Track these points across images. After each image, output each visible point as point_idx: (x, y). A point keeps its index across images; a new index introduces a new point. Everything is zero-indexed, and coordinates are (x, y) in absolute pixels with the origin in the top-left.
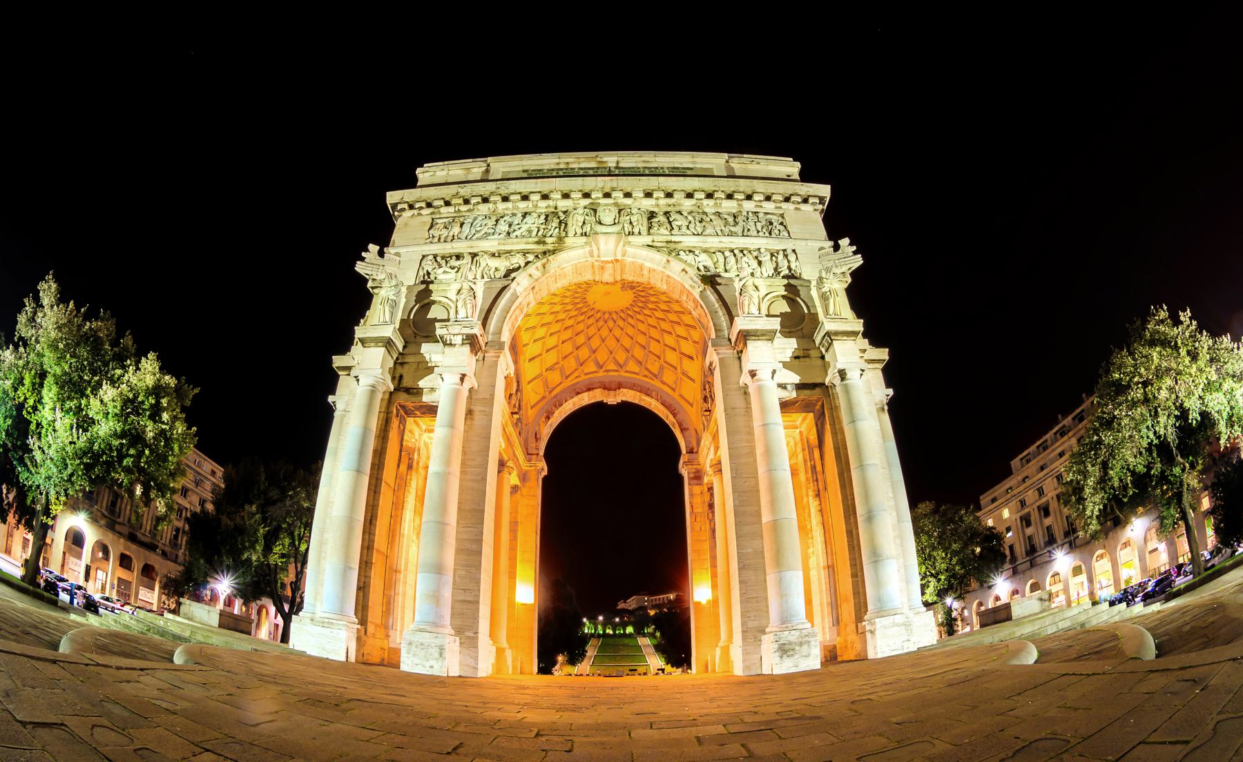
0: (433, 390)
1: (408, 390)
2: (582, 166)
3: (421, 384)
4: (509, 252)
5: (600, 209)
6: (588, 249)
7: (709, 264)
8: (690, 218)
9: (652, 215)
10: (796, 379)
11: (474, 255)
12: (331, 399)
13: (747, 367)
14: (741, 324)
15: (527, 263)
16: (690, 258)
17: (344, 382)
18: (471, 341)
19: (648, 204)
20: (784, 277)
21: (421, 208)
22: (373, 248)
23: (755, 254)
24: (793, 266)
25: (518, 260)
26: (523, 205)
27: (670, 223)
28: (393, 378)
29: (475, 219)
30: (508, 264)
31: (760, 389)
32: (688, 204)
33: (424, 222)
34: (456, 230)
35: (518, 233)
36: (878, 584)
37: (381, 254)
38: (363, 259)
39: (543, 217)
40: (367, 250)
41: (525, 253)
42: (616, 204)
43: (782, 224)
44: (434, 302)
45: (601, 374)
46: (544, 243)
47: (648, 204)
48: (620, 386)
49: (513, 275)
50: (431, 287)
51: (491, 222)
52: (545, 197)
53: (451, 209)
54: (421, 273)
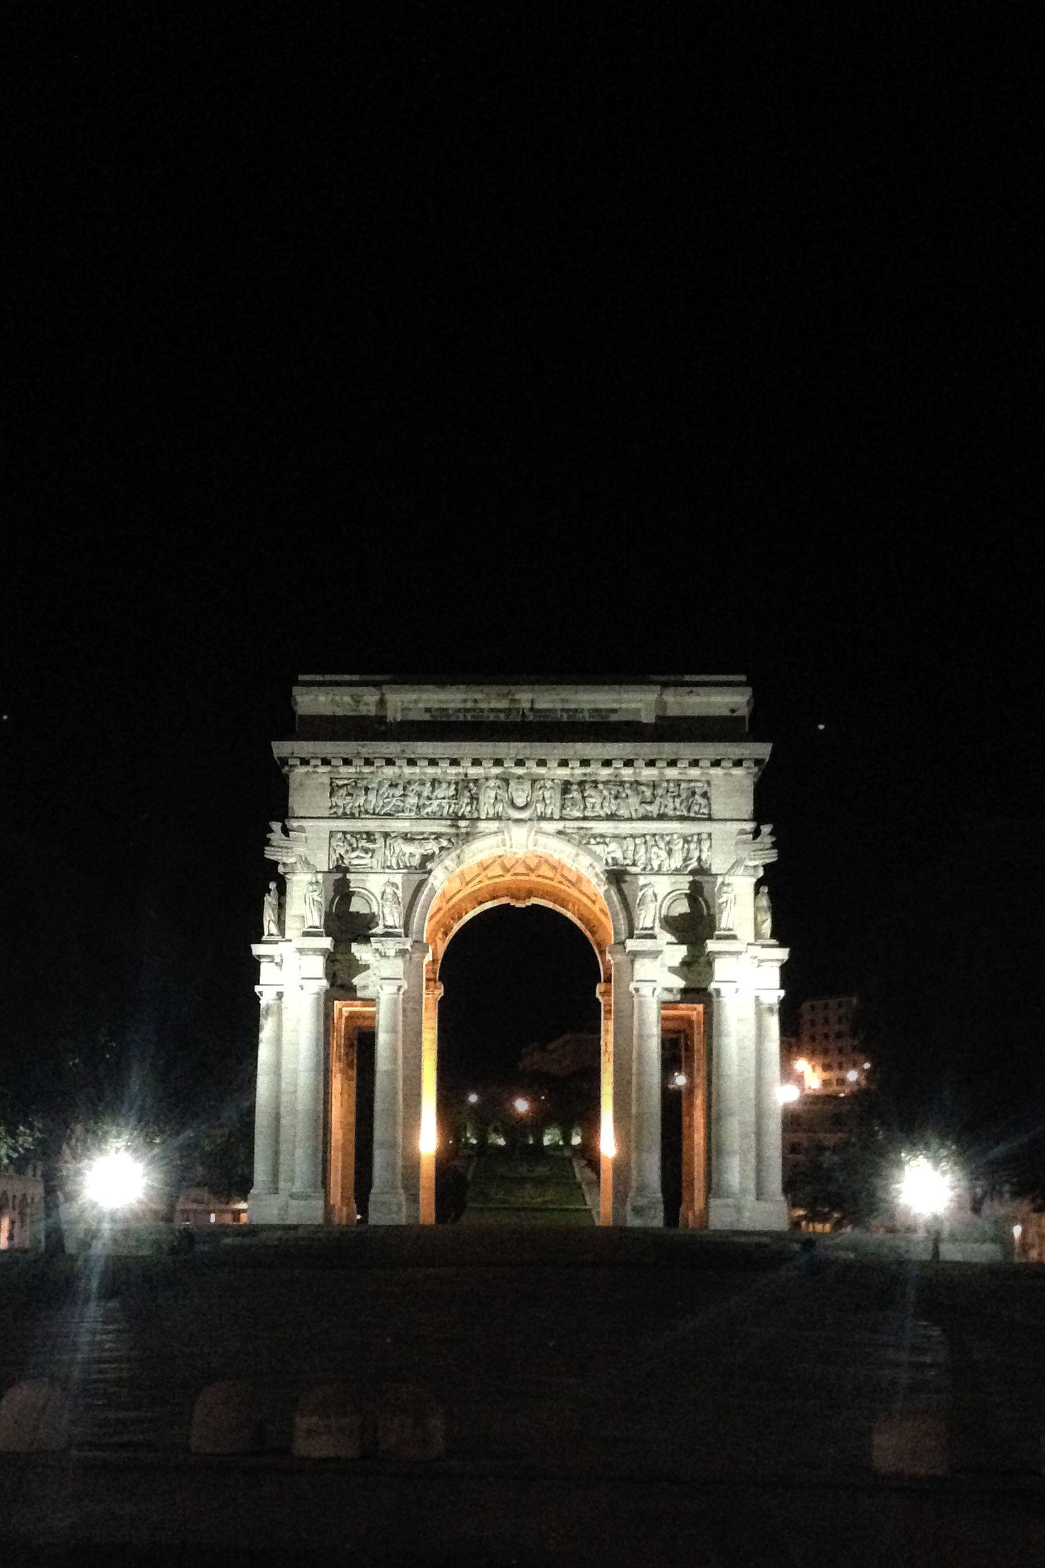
0: (365, 987)
1: (342, 986)
2: (493, 705)
3: (357, 981)
4: (422, 833)
5: (512, 784)
6: (500, 837)
7: (619, 855)
8: (605, 792)
9: (566, 787)
10: (680, 983)
11: (386, 835)
12: (257, 989)
13: (632, 986)
14: (631, 945)
15: (442, 849)
16: (599, 849)
17: (265, 969)
18: (402, 953)
19: (563, 773)
20: (692, 873)
21: (315, 766)
22: (276, 826)
23: (667, 839)
24: (704, 857)
25: (432, 847)
26: (431, 770)
27: (584, 798)
28: (327, 975)
29: (380, 784)
30: (422, 851)
31: (641, 1004)
32: (605, 773)
33: (323, 784)
34: (361, 801)
35: (429, 810)
36: (720, 1173)
37: (286, 831)
38: (267, 843)
39: (453, 787)
40: (272, 831)
41: (438, 836)
42: (530, 774)
43: (705, 795)
44: (354, 893)
45: (508, 877)
46: (458, 827)
47: (563, 773)
48: (530, 894)
49: (429, 866)
50: (349, 876)
51: (399, 792)
52: (454, 762)
53: (352, 770)
54: (334, 857)
